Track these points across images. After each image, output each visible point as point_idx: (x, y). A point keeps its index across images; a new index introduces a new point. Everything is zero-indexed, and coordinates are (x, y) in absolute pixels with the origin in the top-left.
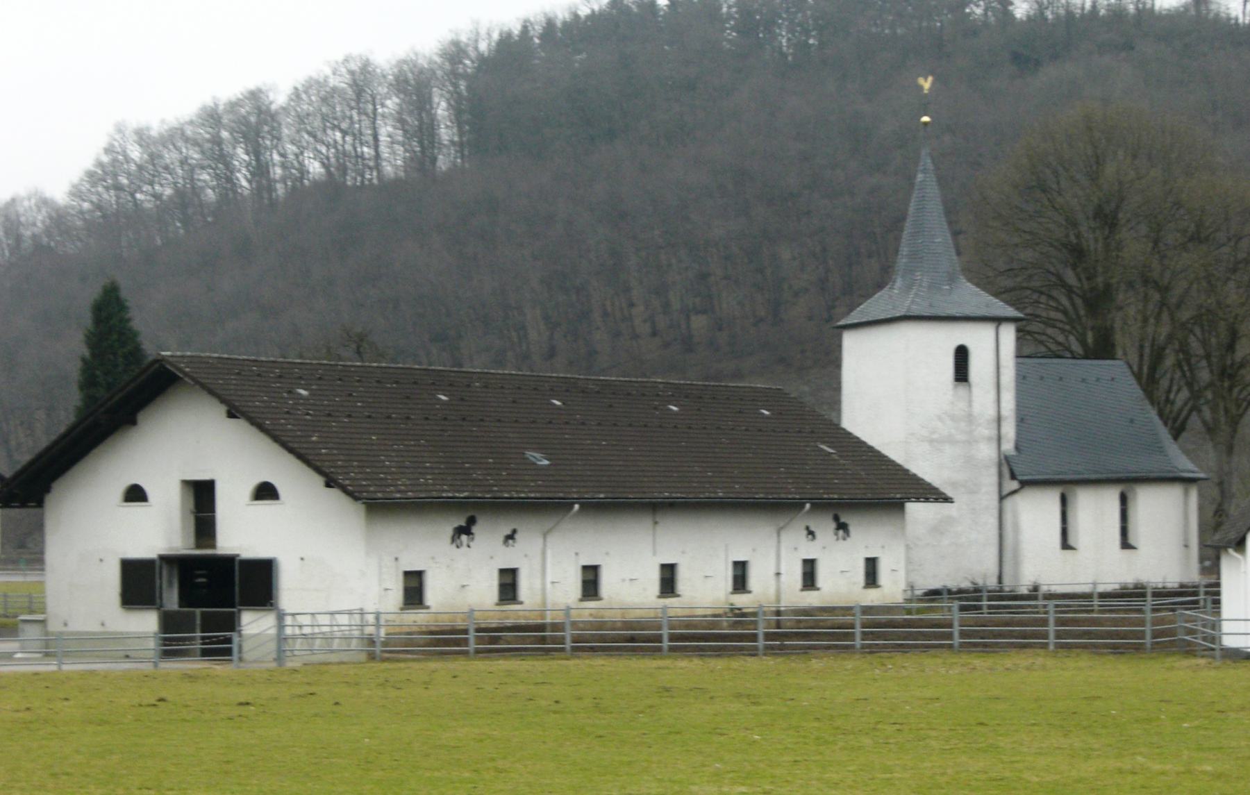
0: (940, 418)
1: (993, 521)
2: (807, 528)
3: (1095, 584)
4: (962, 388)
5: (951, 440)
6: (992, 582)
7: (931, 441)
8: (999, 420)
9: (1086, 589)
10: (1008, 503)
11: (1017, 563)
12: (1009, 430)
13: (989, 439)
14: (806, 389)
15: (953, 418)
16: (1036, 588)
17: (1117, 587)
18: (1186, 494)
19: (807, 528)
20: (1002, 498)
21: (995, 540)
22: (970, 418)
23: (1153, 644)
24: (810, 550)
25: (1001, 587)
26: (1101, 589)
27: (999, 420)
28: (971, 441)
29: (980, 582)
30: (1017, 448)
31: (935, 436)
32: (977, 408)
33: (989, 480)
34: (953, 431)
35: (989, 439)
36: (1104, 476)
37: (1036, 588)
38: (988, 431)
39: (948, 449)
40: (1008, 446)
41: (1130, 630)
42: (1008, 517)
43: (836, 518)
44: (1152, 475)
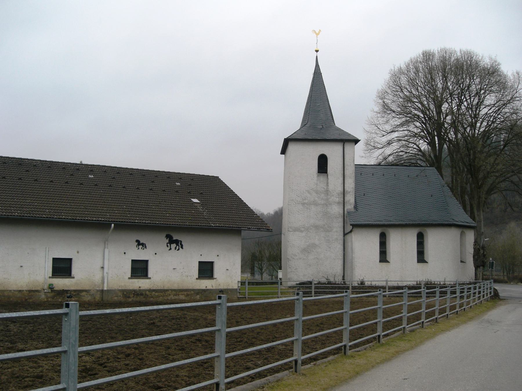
0: (309, 192)
1: (340, 247)
2: (138, 241)
3: (387, 281)
4: (322, 177)
5: (315, 204)
6: (339, 279)
7: (303, 204)
8: (344, 193)
9: (383, 284)
10: (348, 237)
11: (352, 269)
12: (350, 198)
13: (339, 203)
14: (497, 229)
15: (317, 192)
16: (362, 283)
17: (415, 283)
18: (462, 234)
19: (138, 241)
20: (345, 234)
21: (341, 257)
22: (327, 192)
23: (341, 324)
24: (141, 255)
25: (344, 282)
26: (390, 284)
27: (344, 193)
28: (327, 204)
29: (332, 280)
30: (356, 207)
31: (306, 201)
32: (331, 187)
33: (338, 225)
34: (316, 199)
35: (339, 203)
36: (404, 223)
37: (362, 283)
38: (336, 198)
39: (313, 208)
40: (350, 206)
41: (418, 313)
42: (348, 245)
43: (168, 237)
44: (434, 223)
